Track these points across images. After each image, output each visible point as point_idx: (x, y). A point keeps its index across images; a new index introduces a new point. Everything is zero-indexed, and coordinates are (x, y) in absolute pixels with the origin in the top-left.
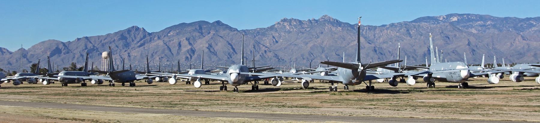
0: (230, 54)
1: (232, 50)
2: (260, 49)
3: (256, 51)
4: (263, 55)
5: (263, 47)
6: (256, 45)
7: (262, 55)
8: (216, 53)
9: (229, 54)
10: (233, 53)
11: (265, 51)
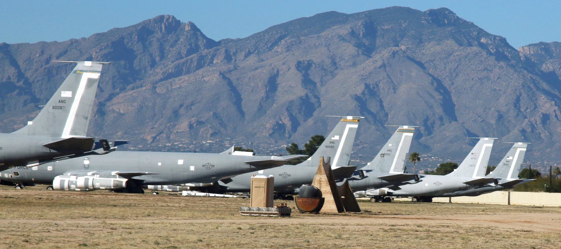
0: (429, 123)
1: (439, 111)
2: (536, 107)
3: (518, 115)
4: (532, 131)
5: (546, 102)
6: (524, 95)
7: (529, 130)
8: (386, 115)
9: (427, 119)
10: (441, 119)
11: (545, 118)
